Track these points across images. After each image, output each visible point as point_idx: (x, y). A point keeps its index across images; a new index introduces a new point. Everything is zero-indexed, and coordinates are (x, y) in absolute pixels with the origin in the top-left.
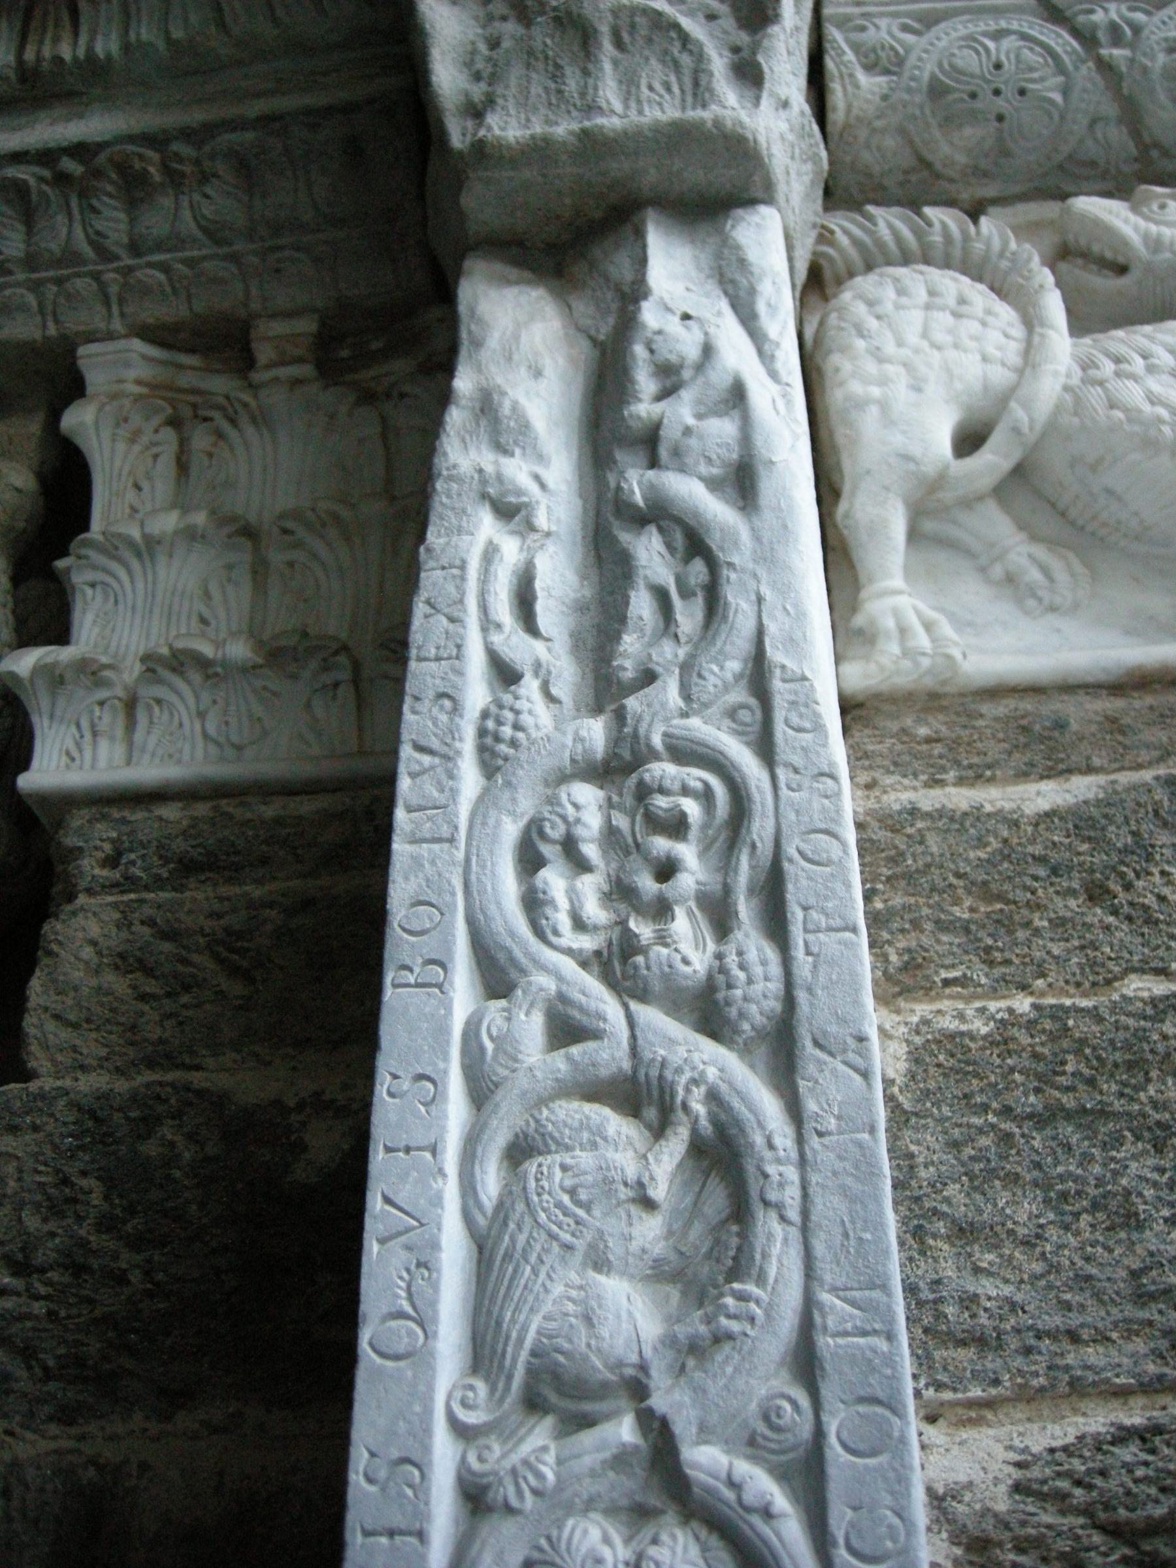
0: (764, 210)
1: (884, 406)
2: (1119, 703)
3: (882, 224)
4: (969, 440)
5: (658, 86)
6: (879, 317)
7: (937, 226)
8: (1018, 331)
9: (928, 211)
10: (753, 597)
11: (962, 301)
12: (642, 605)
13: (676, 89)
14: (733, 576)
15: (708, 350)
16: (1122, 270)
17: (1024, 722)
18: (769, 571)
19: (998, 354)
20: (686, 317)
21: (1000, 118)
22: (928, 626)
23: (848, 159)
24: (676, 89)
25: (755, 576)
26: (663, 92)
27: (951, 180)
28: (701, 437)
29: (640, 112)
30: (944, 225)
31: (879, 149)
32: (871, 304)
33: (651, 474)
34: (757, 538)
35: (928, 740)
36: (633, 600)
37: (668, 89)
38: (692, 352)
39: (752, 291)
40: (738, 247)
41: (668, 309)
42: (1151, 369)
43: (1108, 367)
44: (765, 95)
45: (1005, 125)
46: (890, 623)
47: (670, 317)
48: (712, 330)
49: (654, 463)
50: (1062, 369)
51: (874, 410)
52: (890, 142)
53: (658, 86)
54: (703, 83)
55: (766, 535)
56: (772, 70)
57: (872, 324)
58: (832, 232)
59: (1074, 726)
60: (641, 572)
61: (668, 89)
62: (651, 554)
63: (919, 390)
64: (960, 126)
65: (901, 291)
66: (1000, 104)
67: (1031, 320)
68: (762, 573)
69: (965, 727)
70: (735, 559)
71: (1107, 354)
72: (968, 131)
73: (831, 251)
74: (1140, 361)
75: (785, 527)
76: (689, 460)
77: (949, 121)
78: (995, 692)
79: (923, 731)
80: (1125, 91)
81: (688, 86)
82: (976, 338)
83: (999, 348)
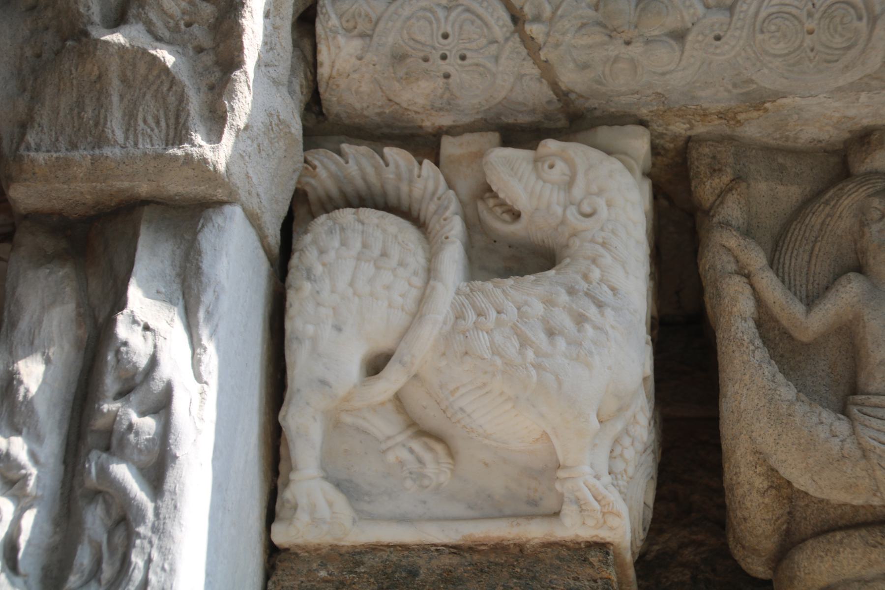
0: (227, 209)
1: (314, 340)
2: (455, 560)
3: (351, 162)
4: (376, 365)
5: (150, 120)
6: (324, 265)
7: (392, 166)
8: (418, 281)
9: (388, 151)
10: (146, 557)
11: (384, 254)
12: (84, 557)
13: (163, 124)
14: (138, 542)
15: (154, 362)
16: (516, 215)
17: (389, 571)
18: (160, 539)
19: (400, 300)
20: (147, 328)
21: (447, 76)
22: (330, 504)
23: (335, 99)
24: (163, 124)
25: (150, 542)
26: (153, 125)
27: (416, 112)
28: (137, 434)
29: (136, 144)
30: (397, 166)
31: (357, 92)
32: (322, 252)
33: (104, 456)
34: (157, 514)
35: (325, 581)
36: (79, 552)
37: (158, 123)
38: (142, 362)
39: (198, 302)
40: (199, 253)
41: (135, 322)
42: (499, 323)
43: (471, 316)
44: (226, 130)
45: (451, 80)
46: (303, 502)
47: (135, 327)
48: (160, 343)
49: (107, 449)
50: (441, 318)
51: (307, 345)
52: (365, 88)
53: (150, 120)
54: (182, 121)
55: (163, 511)
56: (233, 109)
57: (318, 269)
58: (314, 168)
59: (422, 576)
60: (87, 532)
61: (158, 123)
62: (95, 520)
63: (338, 329)
64: (417, 79)
65: (343, 244)
66: (445, 67)
67: (431, 272)
68: (155, 541)
69: (351, 572)
70: (141, 530)
71: (474, 307)
72: (423, 84)
73: (313, 181)
74: (493, 314)
75: (175, 507)
76: (128, 451)
77: (409, 78)
78: (374, 548)
79: (323, 574)
80: (543, 58)
81: (172, 121)
82: (388, 288)
83: (403, 296)
